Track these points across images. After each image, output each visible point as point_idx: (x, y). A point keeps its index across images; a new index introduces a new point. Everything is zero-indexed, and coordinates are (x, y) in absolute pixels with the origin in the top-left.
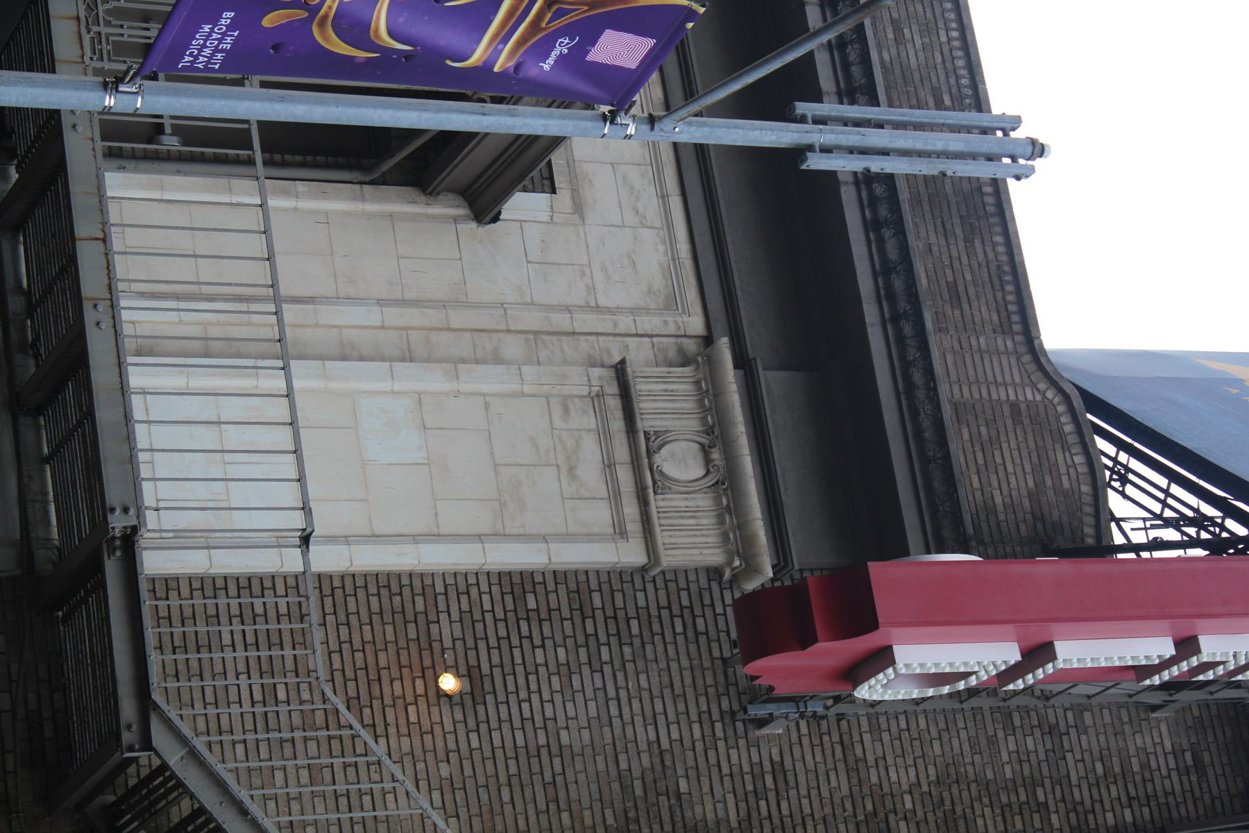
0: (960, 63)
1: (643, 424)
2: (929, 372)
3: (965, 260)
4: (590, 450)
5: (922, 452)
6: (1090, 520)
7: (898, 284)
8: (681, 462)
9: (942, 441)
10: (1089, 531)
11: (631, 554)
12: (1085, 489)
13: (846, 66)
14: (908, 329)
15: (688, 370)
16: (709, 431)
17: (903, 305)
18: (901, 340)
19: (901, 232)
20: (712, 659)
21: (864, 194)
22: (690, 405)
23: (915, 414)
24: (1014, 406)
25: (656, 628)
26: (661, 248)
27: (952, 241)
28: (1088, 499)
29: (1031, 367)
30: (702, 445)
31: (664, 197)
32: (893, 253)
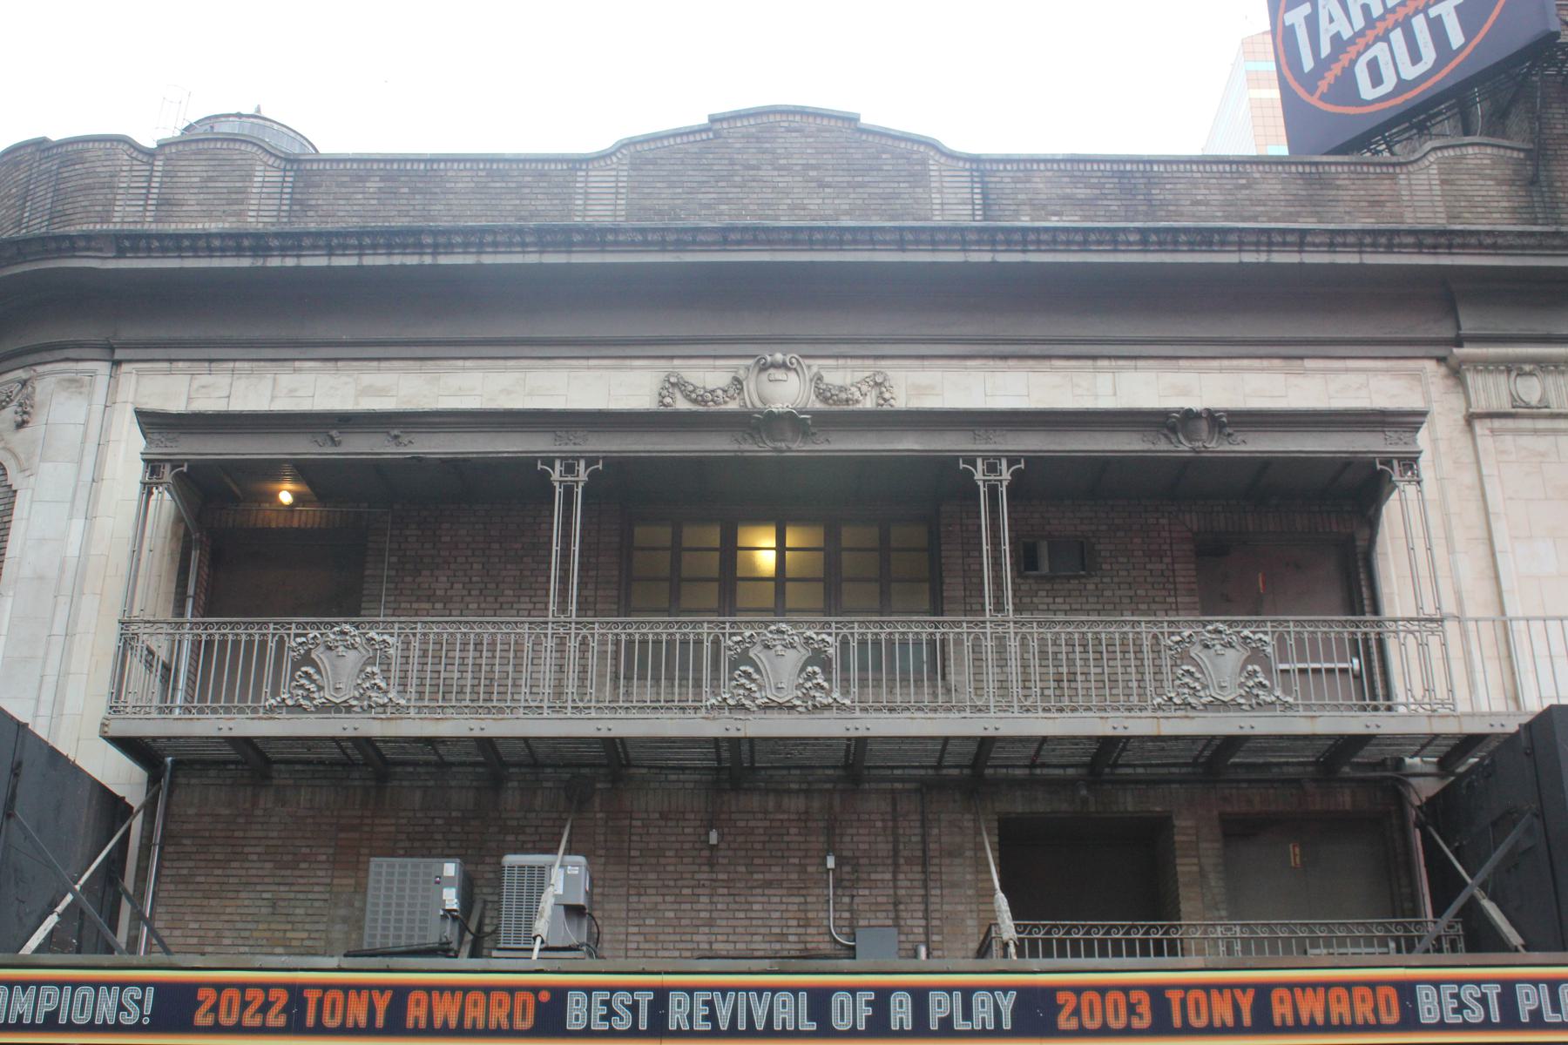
0: (1215, 168)
1: (1507, 408)
2: (1488, 233)
4: (1527, 441)
5: (1533, 247)
7: (1429, 241)
8: (1531, 389)
10: (1515, 154)
12: (1489, 150)
14: (1458, 240)
15: (1470, 378)
16: (1509, 371)
17: (1443, 240)
18: (1463, 246)
19: (1398, 232)
22: (1490, 380)
23: (1511, 247)
24: (1443, 182)
28: (1495, 151)
29: (1416, 167)
31: (1347, 370)
32: (1410, 240)
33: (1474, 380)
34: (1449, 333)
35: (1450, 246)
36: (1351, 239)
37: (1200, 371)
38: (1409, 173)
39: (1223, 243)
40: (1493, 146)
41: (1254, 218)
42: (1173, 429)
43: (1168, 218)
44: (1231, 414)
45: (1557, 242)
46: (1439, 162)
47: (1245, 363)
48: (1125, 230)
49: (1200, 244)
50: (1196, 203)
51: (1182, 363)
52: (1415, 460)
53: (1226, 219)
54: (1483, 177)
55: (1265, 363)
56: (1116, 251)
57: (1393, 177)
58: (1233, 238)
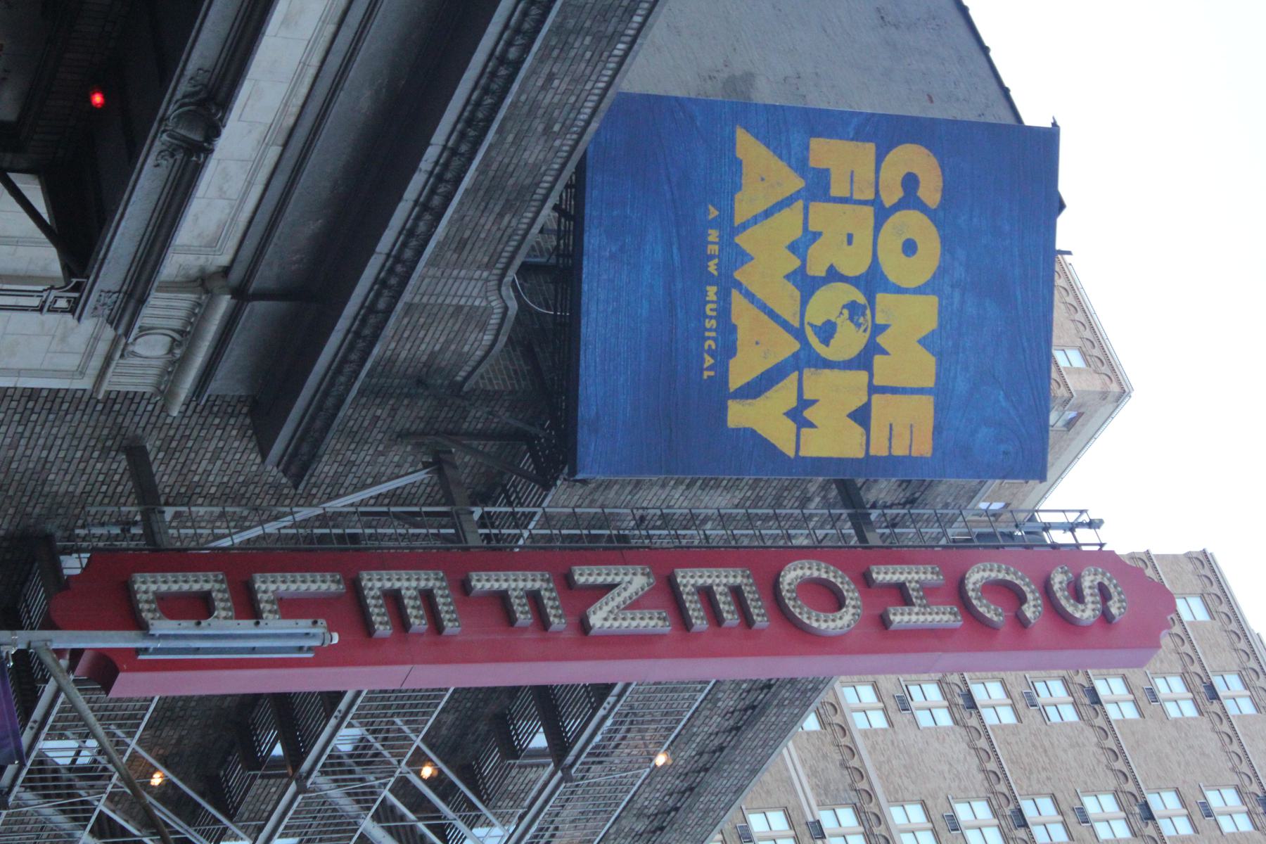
3: (487, 227)
5: (322, 401)
6: (468, 369)
9: (338, 407)
10: (463, 374)
11: (86, 383)
12: (479, 353)
13: (433, 192)
14: (361, 344)
16: (182, 332)
17: (367, 332)
20: (114, 423)
21: (388, 264)
22: (183, 313)
24: (459, 308)
25: (82, 407)
26: (227, 211)
27: (486, 214)
30: (174, 340)
31: (250, 184)
32: (381, 305)
33: (182, 303)
34: (255, 285)
35: (358, 334)
36: (408, 254)
37: (312, 44)
38: (487, 280)
39: (463, 135)
40: (500, 325)
41: (500, 131)
42: (200, 103)
43: (545, 45)
44: (198, 170)
45: (318, 424)
46: (488, 311)
47: (304, 90)
48: (526, 48)
49: (473, 113)
50: (551, 77)
51: (331, 28)
52: (72, 311)
53: (514, 105)
54: (448, 343)
55: (294, 110)
56: (506, 26)
57: (489, 266)
58: (464, 148)
